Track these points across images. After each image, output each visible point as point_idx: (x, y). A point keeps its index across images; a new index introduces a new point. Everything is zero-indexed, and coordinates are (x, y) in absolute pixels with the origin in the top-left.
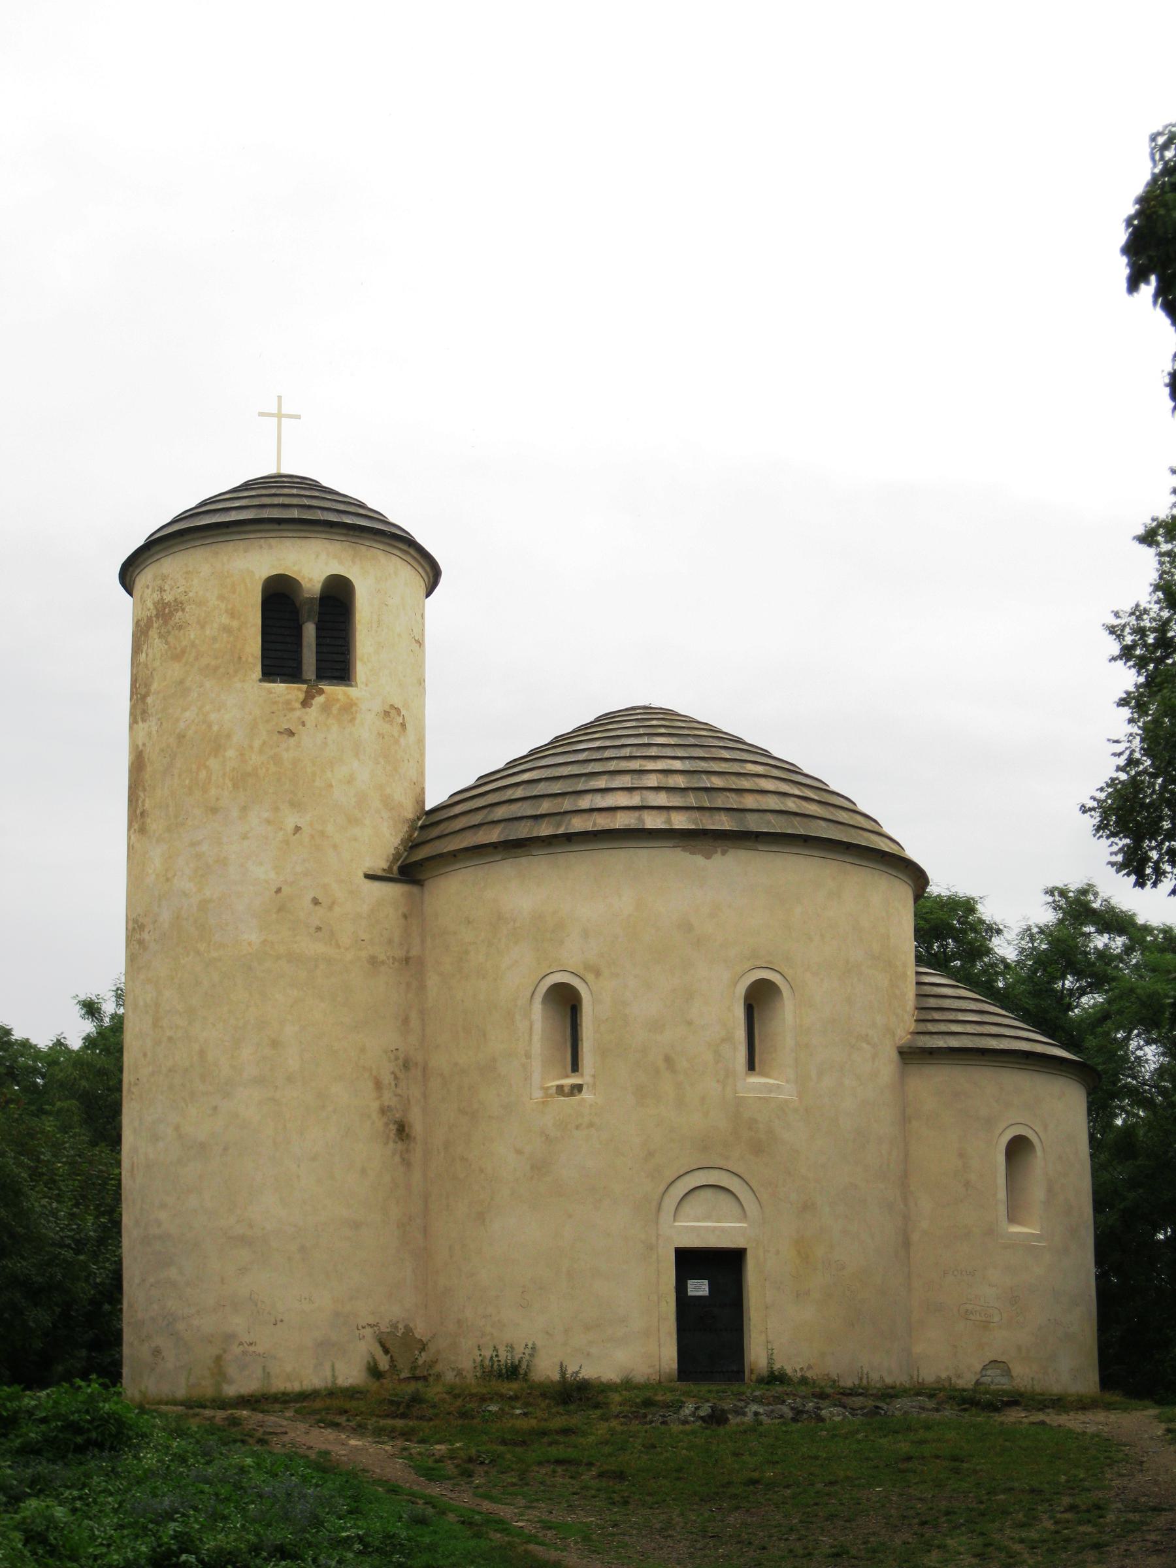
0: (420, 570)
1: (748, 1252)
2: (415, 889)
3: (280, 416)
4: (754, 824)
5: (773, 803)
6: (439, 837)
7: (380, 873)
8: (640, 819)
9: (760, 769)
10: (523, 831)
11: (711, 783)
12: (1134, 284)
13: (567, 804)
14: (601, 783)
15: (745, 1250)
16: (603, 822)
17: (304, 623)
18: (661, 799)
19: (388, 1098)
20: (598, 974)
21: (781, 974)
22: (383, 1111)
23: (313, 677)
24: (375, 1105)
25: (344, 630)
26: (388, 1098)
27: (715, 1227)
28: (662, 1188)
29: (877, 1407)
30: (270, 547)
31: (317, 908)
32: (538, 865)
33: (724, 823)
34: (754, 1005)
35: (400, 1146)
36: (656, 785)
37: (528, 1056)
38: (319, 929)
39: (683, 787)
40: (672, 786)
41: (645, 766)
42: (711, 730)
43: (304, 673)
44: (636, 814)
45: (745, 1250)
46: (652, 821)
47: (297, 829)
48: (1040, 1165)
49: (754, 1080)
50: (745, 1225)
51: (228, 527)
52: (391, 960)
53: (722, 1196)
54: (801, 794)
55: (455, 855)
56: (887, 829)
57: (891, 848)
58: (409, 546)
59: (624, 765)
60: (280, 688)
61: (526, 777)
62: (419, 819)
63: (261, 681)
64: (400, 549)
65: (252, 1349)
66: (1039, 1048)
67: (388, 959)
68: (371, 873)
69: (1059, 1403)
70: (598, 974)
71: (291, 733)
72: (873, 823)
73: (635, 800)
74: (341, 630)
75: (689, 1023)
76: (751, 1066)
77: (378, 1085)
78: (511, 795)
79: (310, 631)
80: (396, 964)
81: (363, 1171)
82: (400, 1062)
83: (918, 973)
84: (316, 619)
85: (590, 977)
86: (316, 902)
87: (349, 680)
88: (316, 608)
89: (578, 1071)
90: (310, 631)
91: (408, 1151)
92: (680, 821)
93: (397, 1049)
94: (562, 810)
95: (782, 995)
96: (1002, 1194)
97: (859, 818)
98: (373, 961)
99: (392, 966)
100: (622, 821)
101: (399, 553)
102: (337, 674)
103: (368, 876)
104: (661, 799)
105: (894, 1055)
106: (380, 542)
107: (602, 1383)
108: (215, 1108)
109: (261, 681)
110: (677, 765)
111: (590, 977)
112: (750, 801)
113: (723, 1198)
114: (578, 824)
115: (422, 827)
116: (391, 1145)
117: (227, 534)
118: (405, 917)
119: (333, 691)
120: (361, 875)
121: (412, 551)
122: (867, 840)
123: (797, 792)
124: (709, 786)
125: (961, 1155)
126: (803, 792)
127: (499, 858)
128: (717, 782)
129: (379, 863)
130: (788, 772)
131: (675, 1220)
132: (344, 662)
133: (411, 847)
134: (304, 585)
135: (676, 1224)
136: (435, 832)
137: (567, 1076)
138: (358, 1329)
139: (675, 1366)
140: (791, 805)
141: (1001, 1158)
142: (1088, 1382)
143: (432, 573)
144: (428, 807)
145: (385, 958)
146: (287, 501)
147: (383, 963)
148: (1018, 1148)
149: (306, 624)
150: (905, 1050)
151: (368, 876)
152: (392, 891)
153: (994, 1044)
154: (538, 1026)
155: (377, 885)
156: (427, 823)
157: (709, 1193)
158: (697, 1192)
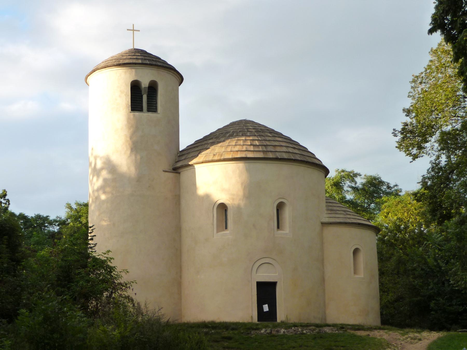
2: (177, 175)
3: (133, 30)
4: (279, 155)
5: (284, 149)
6: (185, 159)
9: (280, 139)
29: (320, 330)
36: (250, 144)
39: (258, 144)
40: (255, 144)
42: (294, 144)
44: (245, 153)
49: (280, 232)
53: (270, 266)
54: (292, 147)
56: (317, 156)
58: (175, 71)
60: (137, 114)
62: (178, 154)
68: (164, 170)
69: (371, 329)
74: (155, 97)
76: (278, 227)
79: (145, 98)
84: (147, 94)
88: (147, 90)
89: (227, 229)
90: (145, 98)
101: (172, 74)
103: (164, 171)
107: (253, 323)
109: (130, 112)
110: (256, 138)
112: (278, 149)
115: (179, 156)
121: (175, 73)
123: (291, 146)
124: (265, 144)
126: (292, 146)
128: (268, 143)
129: (167, 167)
135: (257, 274)
136: (183, 158)
137: (224, 231)
140: (291, 150)
142: (378, 322)
143: (181, 79)
144: (180, 150)
148: (356, 251)
152: (171, 175)
154: (215, 215)
155: (167, 173)
157: (266, 265)
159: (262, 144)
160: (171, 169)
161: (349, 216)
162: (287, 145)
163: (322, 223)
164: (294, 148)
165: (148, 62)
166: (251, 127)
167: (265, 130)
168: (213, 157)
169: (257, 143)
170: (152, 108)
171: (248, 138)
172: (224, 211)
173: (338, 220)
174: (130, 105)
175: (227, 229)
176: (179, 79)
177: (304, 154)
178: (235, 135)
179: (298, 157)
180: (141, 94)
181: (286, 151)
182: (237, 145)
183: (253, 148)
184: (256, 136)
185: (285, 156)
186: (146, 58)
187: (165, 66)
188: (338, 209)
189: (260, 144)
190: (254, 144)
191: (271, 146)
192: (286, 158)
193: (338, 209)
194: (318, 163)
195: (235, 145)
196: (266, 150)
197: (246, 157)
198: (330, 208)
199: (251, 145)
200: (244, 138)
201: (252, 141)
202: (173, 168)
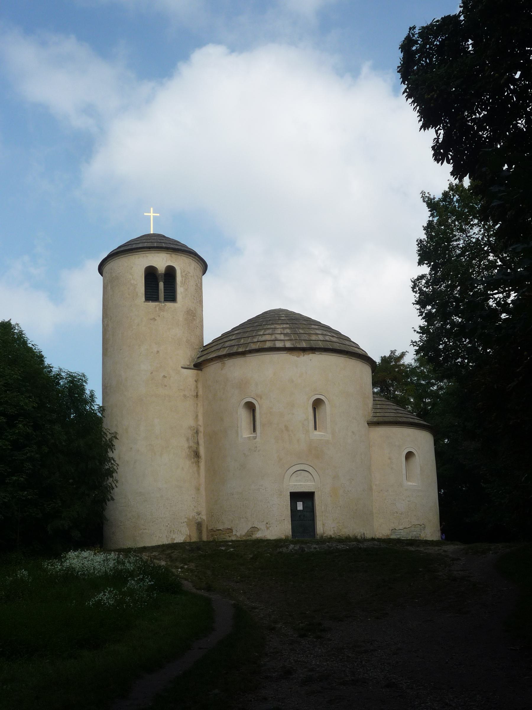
0: (200, 264)
1: (316, 494)
2: (199, 372)
4: (313, 344)
5: (321, 337)
7: (187, 366)
8: (275, 344)
9: (316, 327)
10: (235, 350)
11: (299, 331)
12: (399, 48)
13: (249, 340)
14: (261, 333)
15: (314, 492)
16: (261, 345)
17: (159, 282)
18: (282, 337)
22: (190, 447)
23: (163, 300)
24: (186, 445)
25: (174, 285)
26: (192, 444)
30: (147, 256)
32: (239, 361)
33: (304, 345)
34: (316, 408)
35: (196, 459)
36: (280, 333)
37: (238, 427)
38: (166, 386)
41: (276, 327)
43: (160, 299)
44: (273, 342)
45: (314, 492)
46: (279, 344)
47: (158, 352)
48: (417, 460)
49: (316, 433)
51: (132, 250)
52: (191, 396)
53: (307, 472)
54: (330, 335)
55: (212, 360)
57: (361, 352)
58: (195, 255)
59: (269, 327)
60: (152, 304)
61: (236, 332)
63: (144, 302)
64: (193, 257)
65: (145, 531)
66: (416, 421)
68: (184, 366)
69: (426, 543)
70: (261, 398)
71: (154, 319)
72: (357, 345)
73: (273, 337)
77: (188, 440)
78: (231, 338)
79: (161, 285)
80: (193, 397)
81: (183, 469)
82: (195, 431)
83: (373, 397)
85: (259, 399)
87: (175, 301)
89: (255, 432)
90: (161, 285)
91: (199, 462)
92: (288, 345)
93: (194, 427)
94: (248, 342)
96: (404, 472)
97: (351, 343)
98: (185, 396)
100: (268, 345)
101: (192, 258)
102: (171, 299)
103: (182, 368)
104: (282, 337)
105: (367, 425)
106: (185, 254)
108: (131, 448)
109: (144, 302)
110: (288, 326)
111: (259, 399)
112: (314, 337)
114: (253, 347)
116: (193, 460)
117: (132, 253)
118: (196, 381)
119: (169, 305)
120: (180, 367)
121: (196, 257)
122: (354, 350)
125: (390, 459)
126: (331, 334)
127: (226, 359)
128: (301, 331)
129: (187, 363)
130: (328, 328)
132: (174, 295)
133: (198, 358)
134: (158, 269)
137: (252, 434)
138: (182, 523)
140: (327, 338)
144: (204, 345)
145: (189, 395)
146: (153, 241)
147: (188, 397)
149: (160, 283)
150: (369, 422)
152: (191, 373)
153: (400, 420)
156: (204, 350)
159: (294, 333)
160: (192, 364)
161: (401, 415)
162: (325, 333)
163: (367, 423)
164: (333, 336)
165: (164, 245)
166: (283, 315)
167: (300, 318)
168: (237, 349)
169: (288, 331)
170: (171, 297)
171: (278, 326)
172: (252, 412)
173: (386, 419)
174: (144, 292)
175: (255, 432)
176: (202, 265)
177: (344, 343)
178: (264, 324)
179: (337, 346)
180: (157, 282)
181: (322, 340)
182: (265, 335)
183: (284, 337)
184: (288, 324)
185: (321, 345)
186: (162, 241)
187: (184, 250)
188: (388, 407)
189: (292, 333)
190: (285, 332)
191: (305, 335)
192: (323, 347)
193: (388, 407)
194: (361, 353)
195: (263, 335)
196: (298, 339)
197: (275, 347)
198: (379, 406)
199: (281, 334)
200: (273, 326)
201: (282, 330)
202: (194, 365)
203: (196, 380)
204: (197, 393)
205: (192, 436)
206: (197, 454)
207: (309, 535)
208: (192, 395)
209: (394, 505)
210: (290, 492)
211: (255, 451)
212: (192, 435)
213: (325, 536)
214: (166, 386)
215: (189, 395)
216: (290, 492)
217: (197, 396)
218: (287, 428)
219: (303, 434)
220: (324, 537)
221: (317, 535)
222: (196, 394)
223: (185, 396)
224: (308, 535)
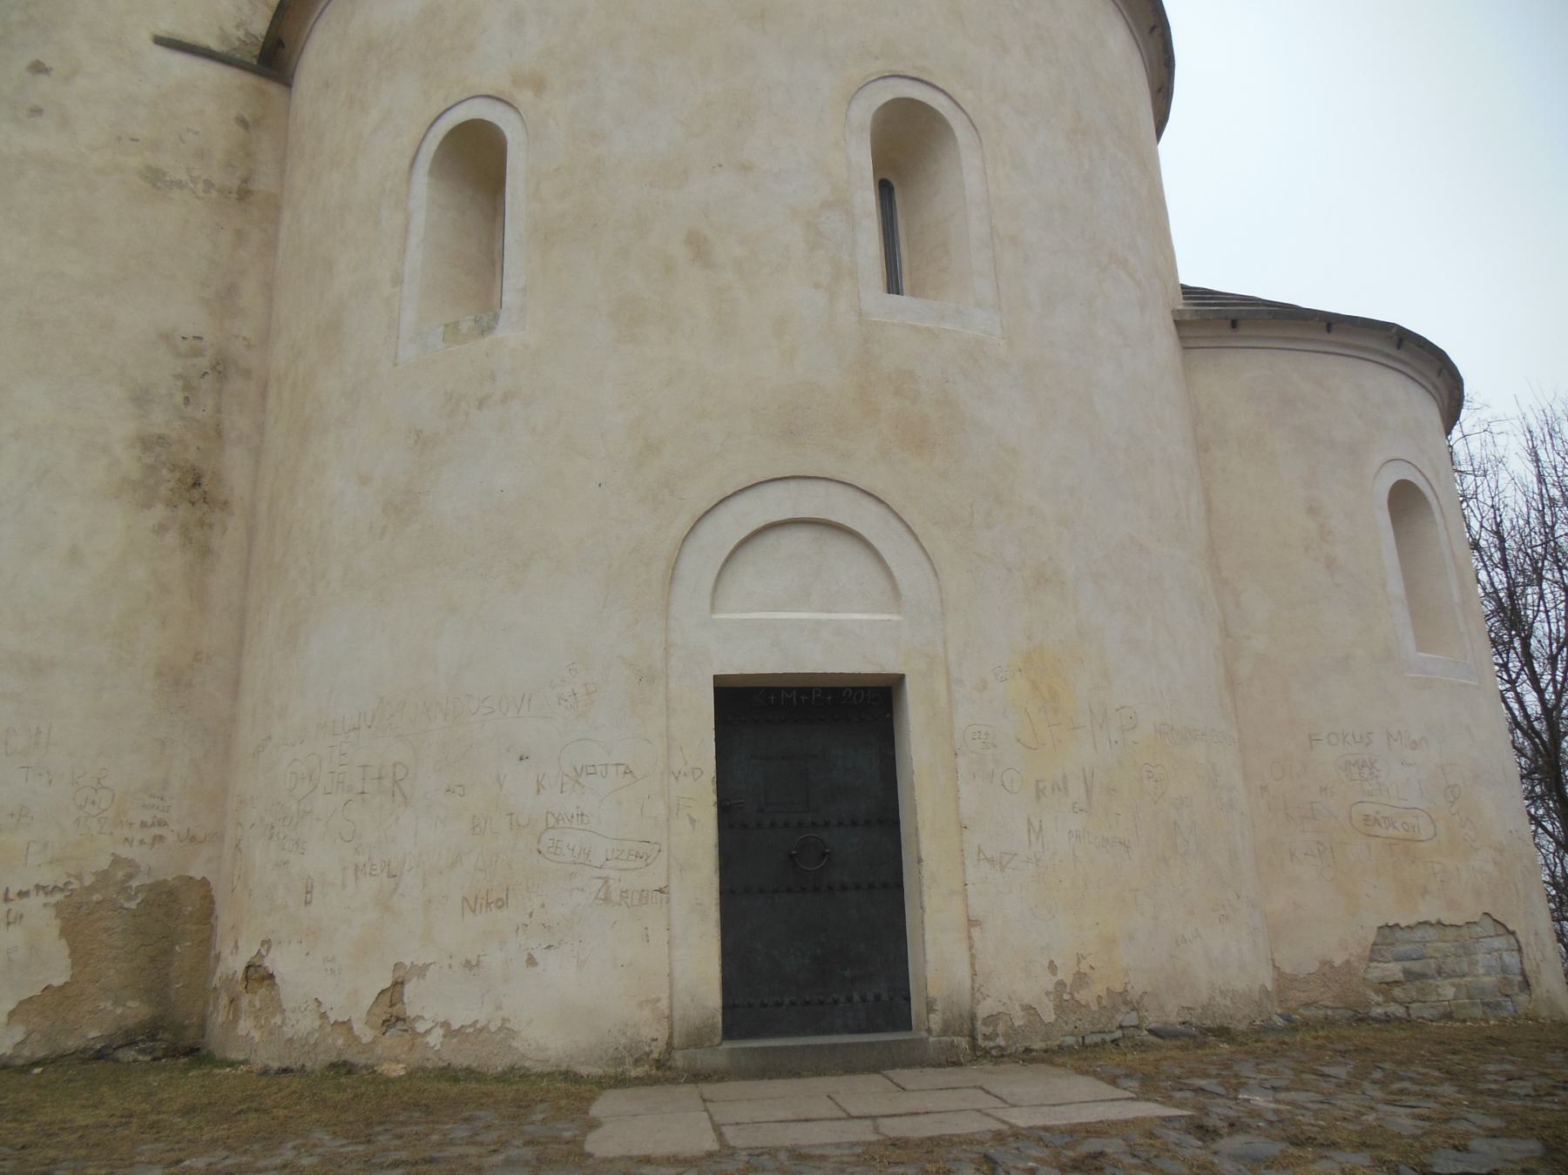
1: (908, 681)
2: (273, 89)
19: (159, 420)
20: (539, 85)
21: (951, 98)
22: (147, 443)
27: (818, 622)
28: (684, 523)
31: (42, 77)
37: (398, 280)
38: (37, 111)
50: (895, 617)
52: (200, 186)
53: (839, 547)
67: (194, 180)
75: (745, 168)
77: (142, 399)
80: (214, 194)
82: (204, 363)
85: (524, 97)
86: (38, 68)
93: (200, 338)
95: (954, 139)
96: (1396, 587)
99: (202, 194)
103: (162, 41)
113: (841, 558)
116: (159, 512)
118: (243, 123)
120: (145, 37)
125: (1312, 510)
131: (713, 608)
135: (714, 617)
139: (711, 997)
141: (1383, 517)
147: (180, 185)
150: (1187, 317)
151: (162, 41)
154: (420, 219)
158: (771, 539)
163: (1175, 321)
203: (248, 119)
204: (245, 181)
205: (180, 383)
206: (205, 481)
207: (864, 999)
208: (209, 184)
209: (1366, 771)
210: (714, 676)
211: (481, 404)
212: (178, 377)
213: (986, 1022)
214: (37, 111)
215: (184, 177)
216: (714, 676)
217: (244, 194)
218: (699, 247)
219: (817, 286)
220: (979, 1023)
221: (930, 1008)
222: (237, 182)
223: (155, 177)
224: (856, 998)
